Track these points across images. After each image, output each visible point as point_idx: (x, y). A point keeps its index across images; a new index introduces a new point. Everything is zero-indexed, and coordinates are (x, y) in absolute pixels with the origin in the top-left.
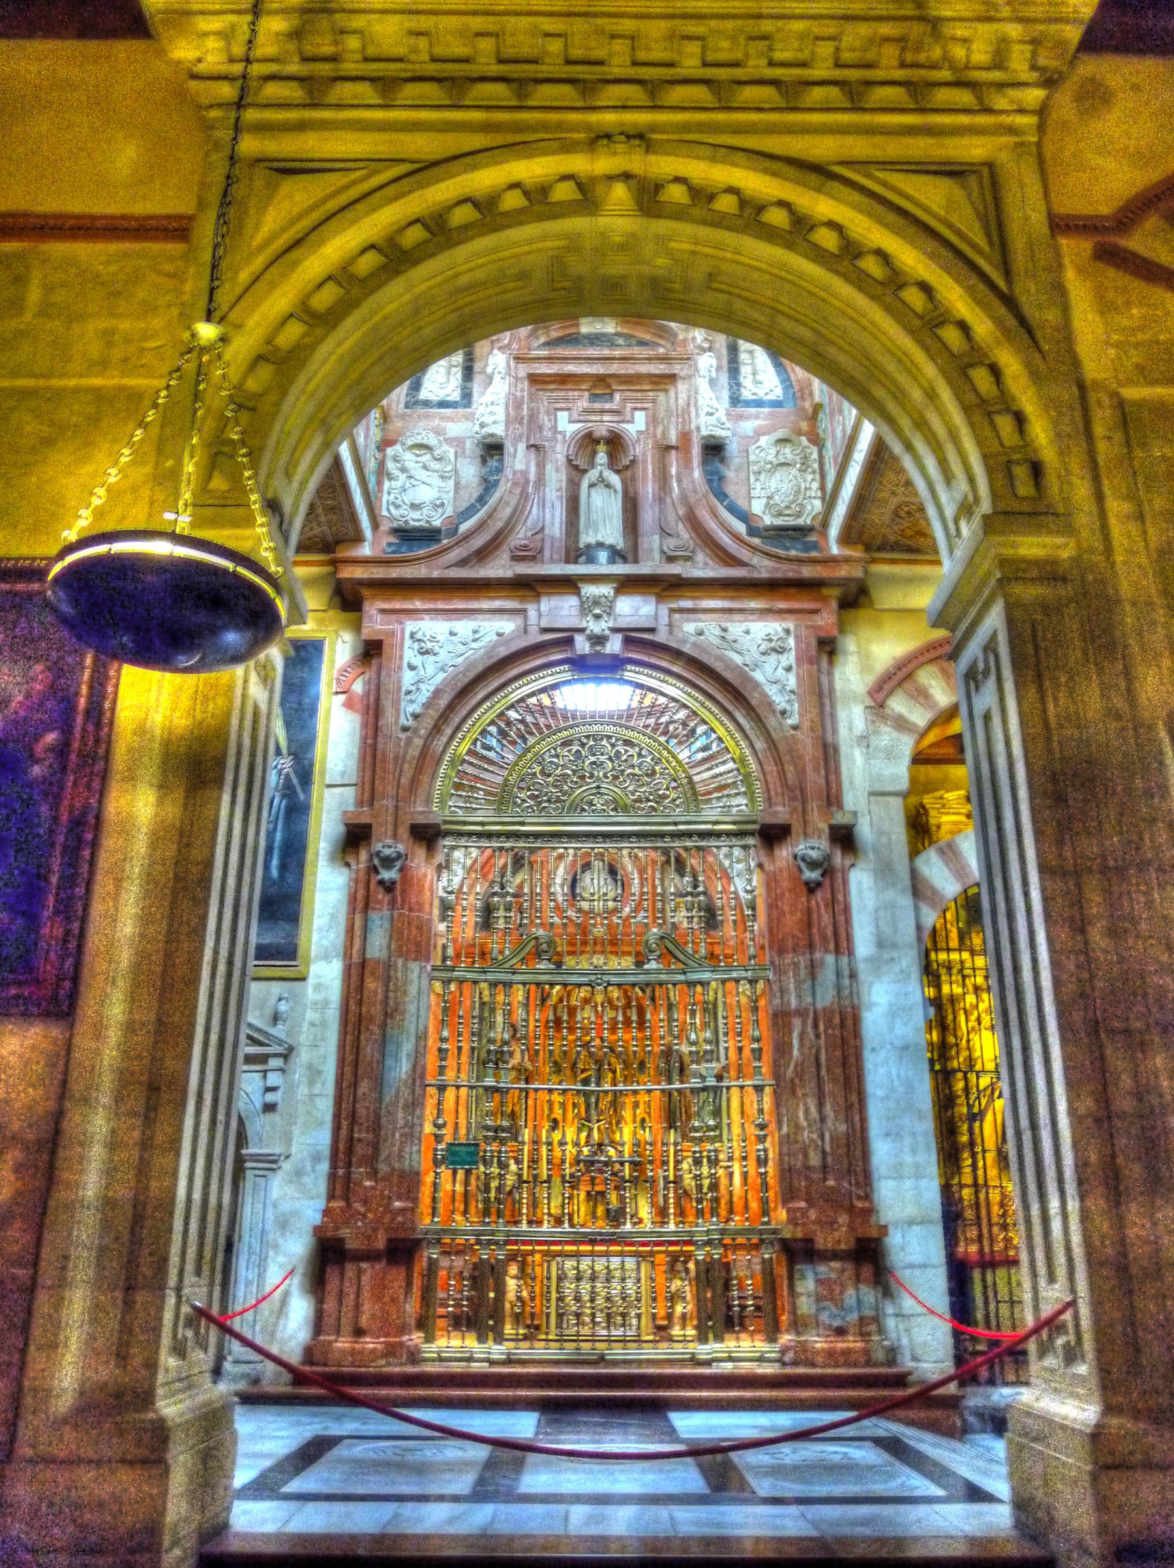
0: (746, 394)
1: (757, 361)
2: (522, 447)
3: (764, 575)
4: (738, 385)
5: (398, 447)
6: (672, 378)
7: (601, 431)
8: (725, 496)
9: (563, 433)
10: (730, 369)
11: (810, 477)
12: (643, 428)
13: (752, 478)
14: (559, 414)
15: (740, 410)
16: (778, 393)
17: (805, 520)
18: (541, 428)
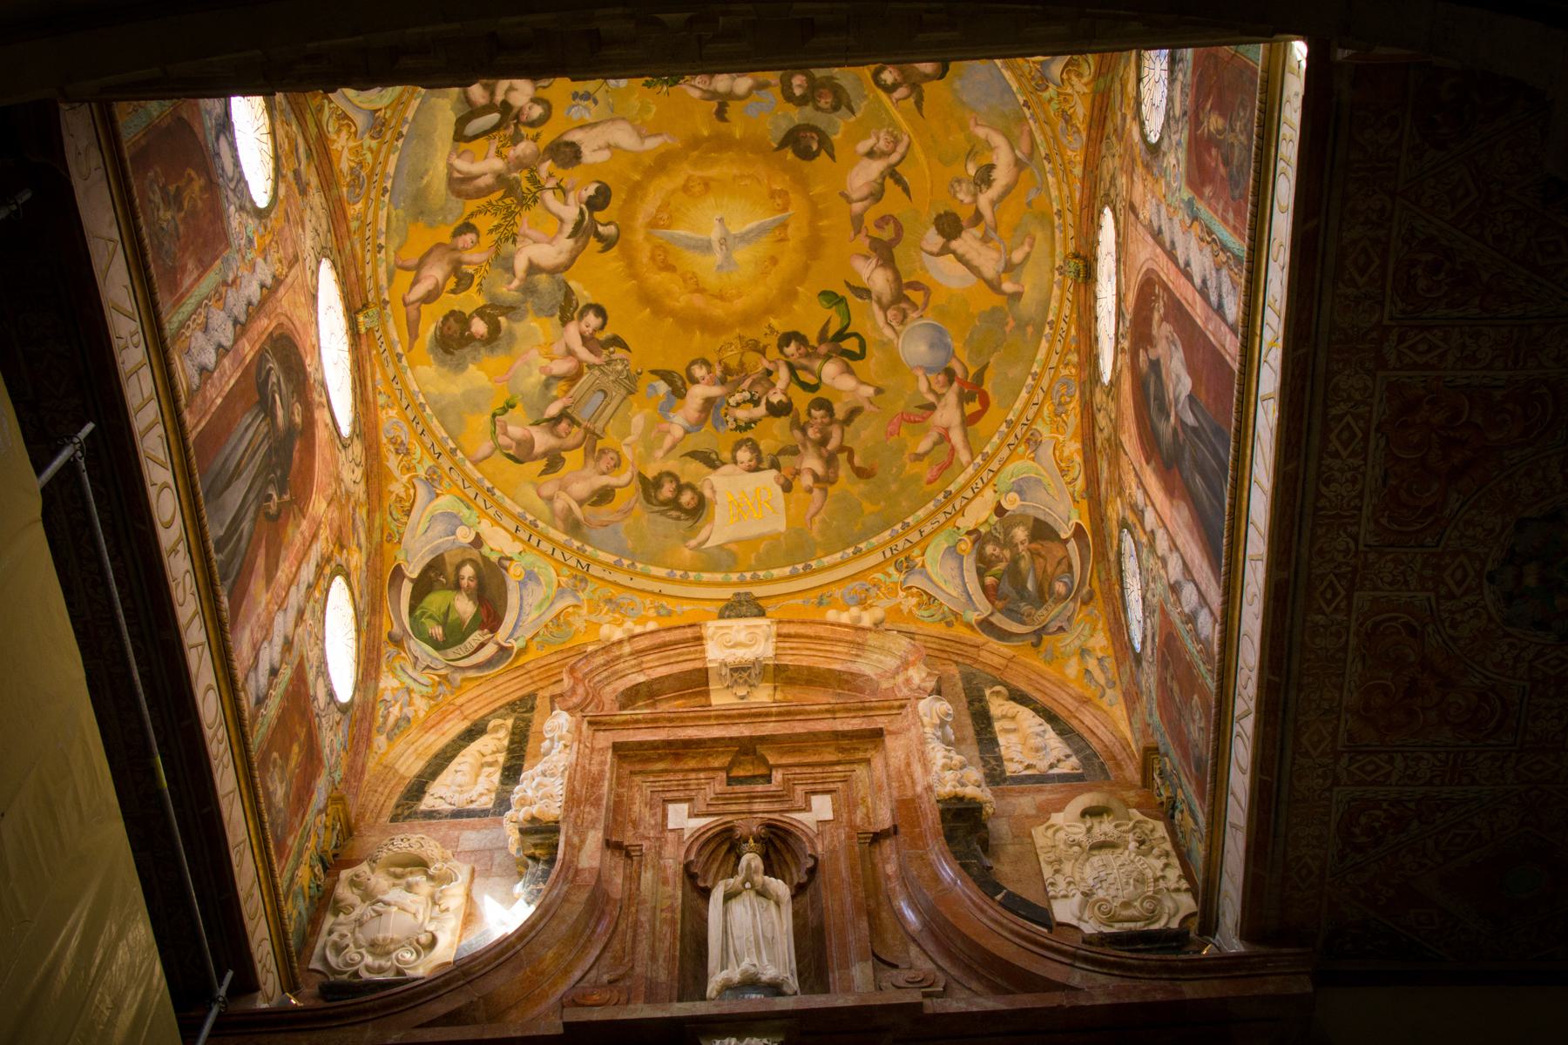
0: (1011, 768)
1: (1025, 724)
2: (594, 838)
3: (1102, 1000)
4: (999, 759)
5: (364, 868)
6: (877, 735)
7: (749, 826)
8: (998, 888)
9: (679, 831)
10: (980, 742)
11: (1159, 864)
12: (829, 816)
13: (1047, 872)
14: (671, 807)
15: (1004, 786)
16: (1070, 765)
17: (1168, 920)
18: (635, 825)
